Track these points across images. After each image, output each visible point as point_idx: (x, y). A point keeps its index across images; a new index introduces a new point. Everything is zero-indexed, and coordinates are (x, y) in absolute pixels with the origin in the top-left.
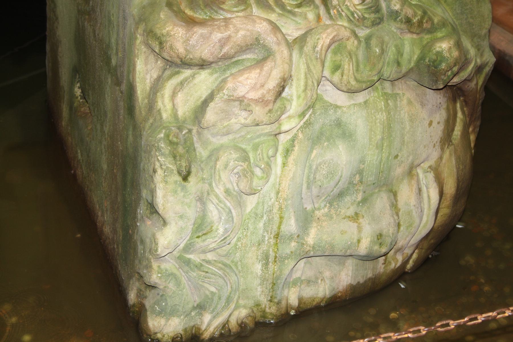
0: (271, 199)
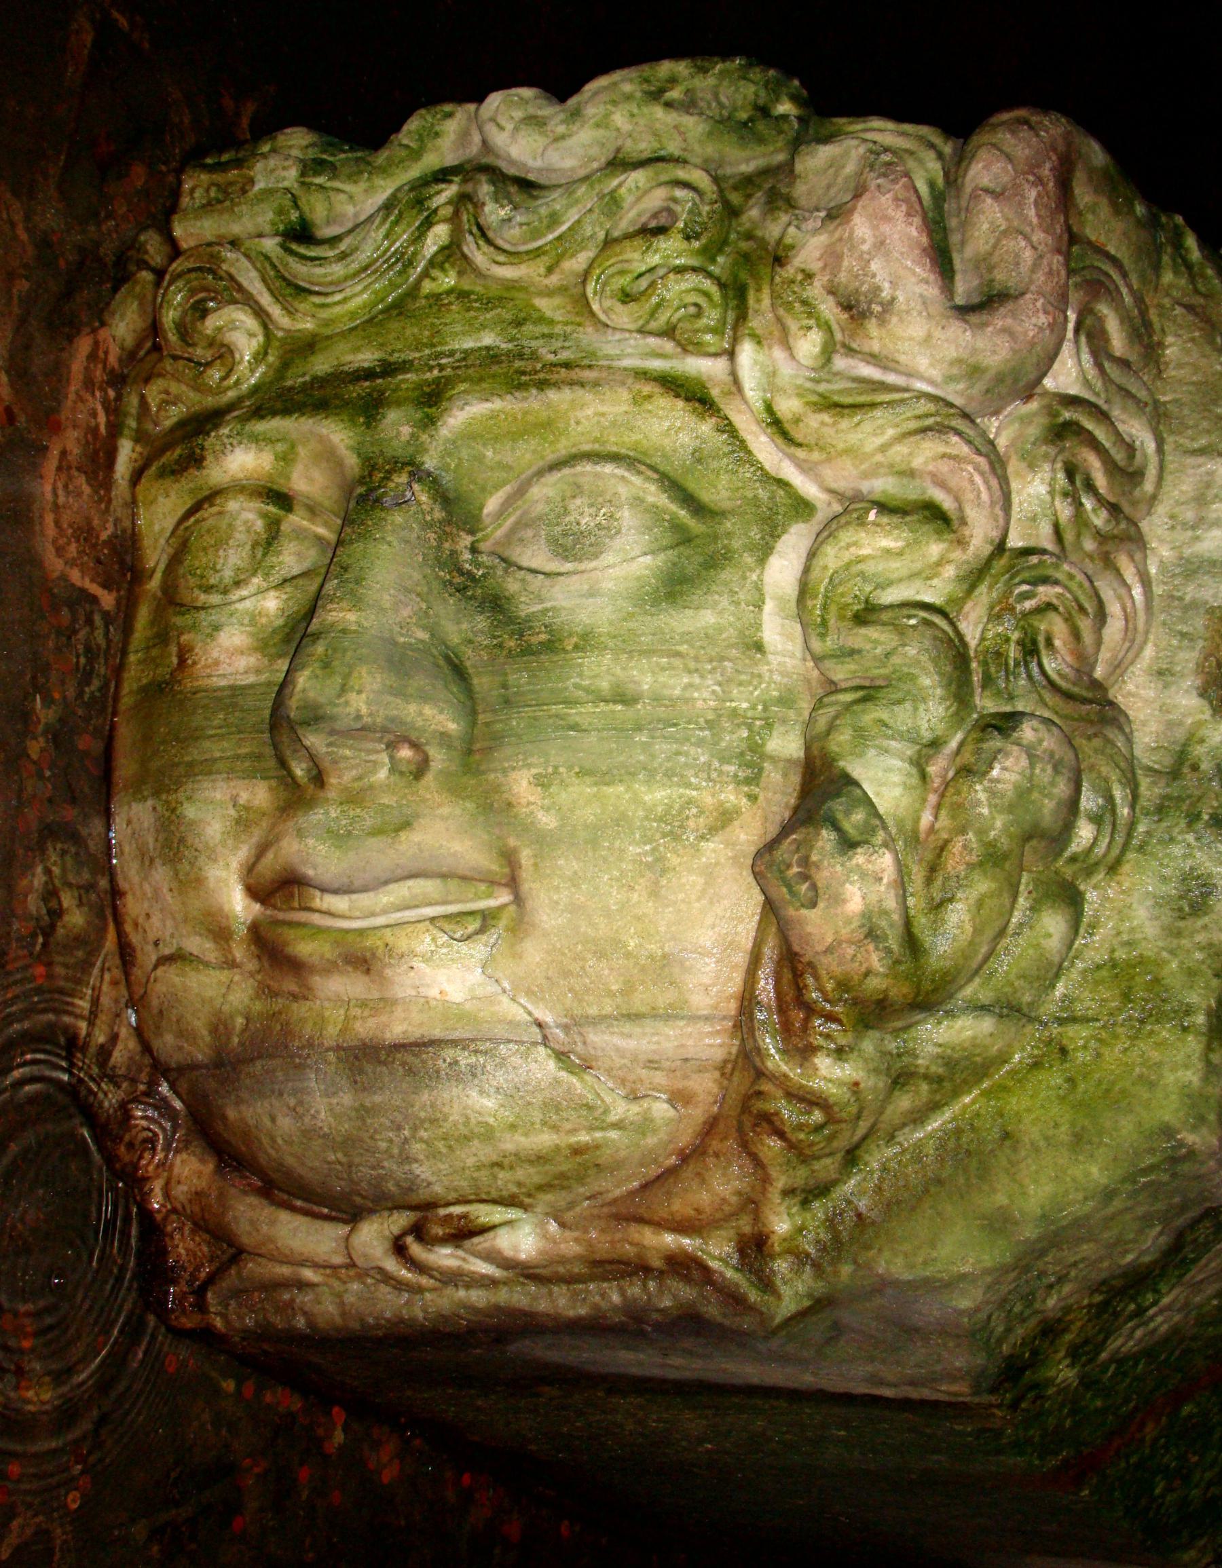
0: (555, 353)
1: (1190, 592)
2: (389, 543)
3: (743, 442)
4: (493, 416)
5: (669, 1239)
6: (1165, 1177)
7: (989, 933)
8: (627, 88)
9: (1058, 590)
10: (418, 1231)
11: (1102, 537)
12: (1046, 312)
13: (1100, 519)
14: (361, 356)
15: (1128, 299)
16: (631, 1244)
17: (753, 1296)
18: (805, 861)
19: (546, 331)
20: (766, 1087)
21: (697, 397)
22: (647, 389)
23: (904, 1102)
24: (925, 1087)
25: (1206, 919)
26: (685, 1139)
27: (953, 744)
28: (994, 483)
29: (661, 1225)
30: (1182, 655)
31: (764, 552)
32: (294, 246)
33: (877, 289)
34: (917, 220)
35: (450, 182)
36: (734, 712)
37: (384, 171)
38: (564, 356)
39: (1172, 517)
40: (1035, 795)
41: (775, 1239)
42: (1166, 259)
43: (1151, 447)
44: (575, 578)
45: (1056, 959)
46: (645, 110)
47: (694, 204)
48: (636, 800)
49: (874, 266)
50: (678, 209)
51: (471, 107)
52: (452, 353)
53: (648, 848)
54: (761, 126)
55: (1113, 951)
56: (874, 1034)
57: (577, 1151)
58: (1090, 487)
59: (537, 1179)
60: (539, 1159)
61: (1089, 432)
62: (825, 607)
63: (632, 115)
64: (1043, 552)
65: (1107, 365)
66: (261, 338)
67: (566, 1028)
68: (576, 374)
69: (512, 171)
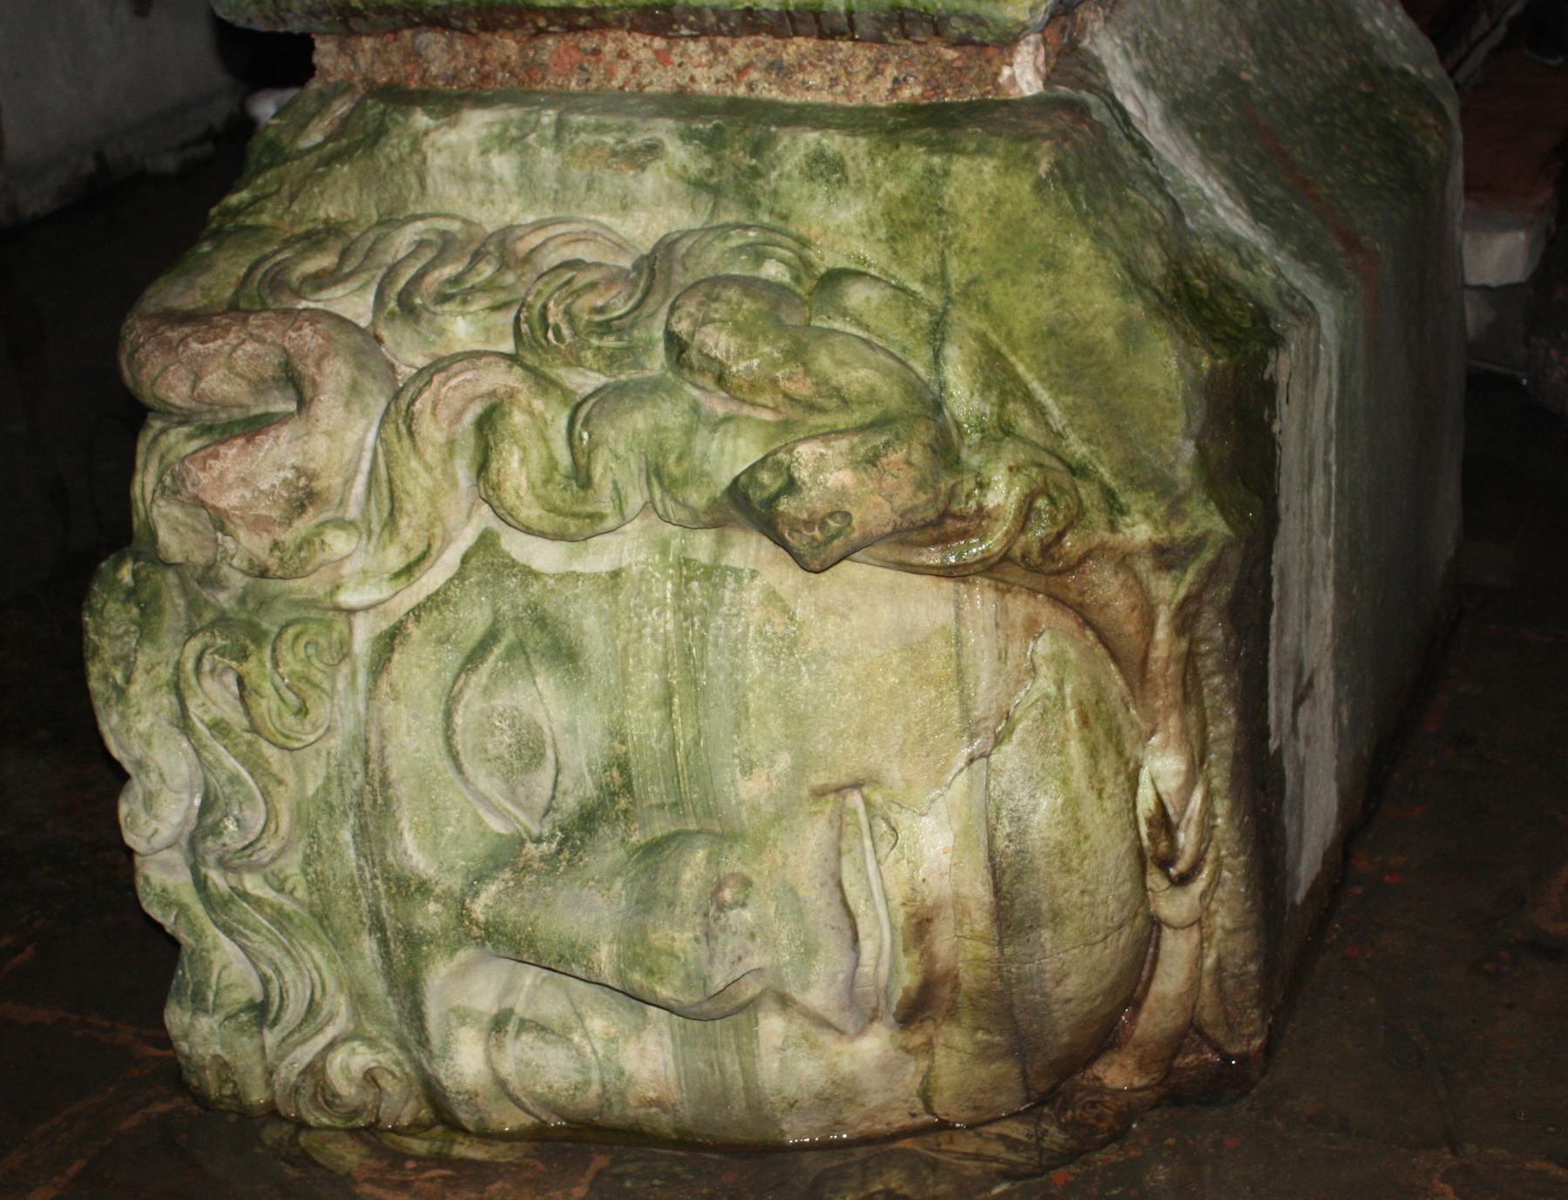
0: (355, 774)
1: (550, 183)
2: (536, 918)
3: (429, 598)
4: (415, 827)
5: (1162, 633)
6: (1081, 187)
7: (867, 352)
8: (115, 719)
9: (551, 304)
10: (1164, 864)
11: (504, 265)
12: (300, 328)
13: (486, 270)
14: (367, 952)
15: (287, 254)
16: (1167, 668)
17: (1208, 555)
18: (809, 524)
19: (336, 783)
20: (1017, 551)
21: (390, 640)
22: (384, 687)
23: (1025, 424)
24: (1011, 406)
25: (847, 158)
26: (1069, 622)
27: (696, 393)
28: (456, 367)
29: (1149, 642)
30: (608, 189)
31: (529, 573)
32: (271, 1016)
33: (285, 482)
34: (223, 449)
35: (206, 877)
36: (677, 595)
37: (199, 936)
38: (358, 766)
39: (482, 203)
40: (740, 318)
41: (1157, 537)
42: (249, 221)
43: (420, 225)
44: (559, 746)
45: (889, 292)
46: (134, 701)
47: (215, 652)
48: (762, 680)
49: (265, 486)
50: (220, 666)
51: (138, 860)
52: (360, 868)
53: (803, 669)
54: (145, 595)
55: (879, 240)
56: (964, 454)
57: (1084, 721)
58: (456, 280)
59: (1112, 757)
60: (1093, 754)
61: (408, 283)
62: (575, 515)
63: (139, 713)
64: (517, 319)
65: (346, 270)
66: (356, 1044)
67: (973, 737)
68: (374, 755)
69: (194, 820)
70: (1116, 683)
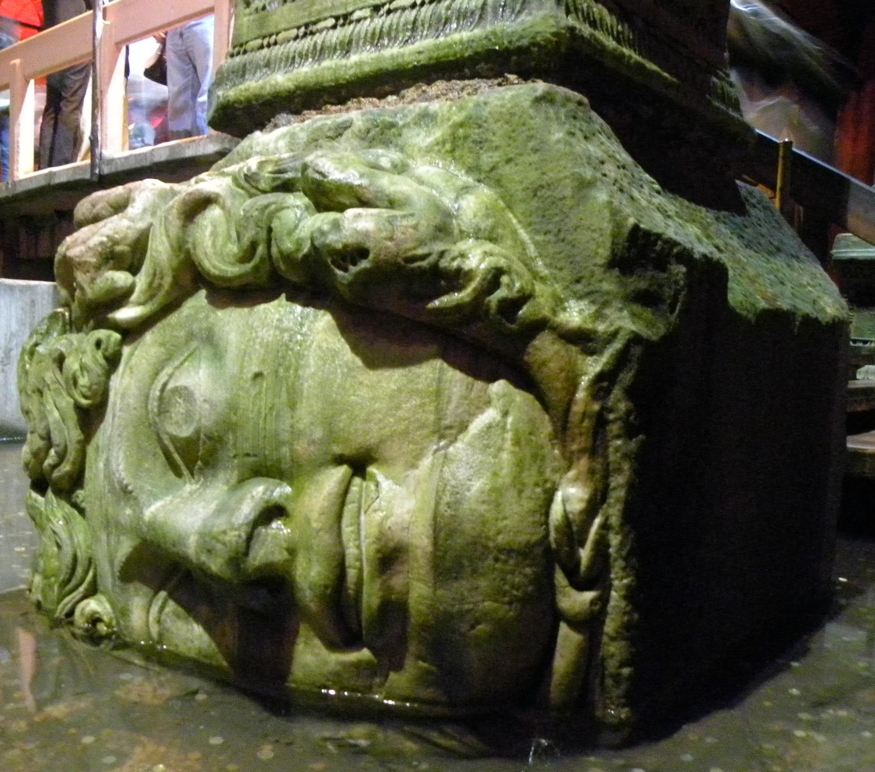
5: (581, 395)
16: (582, 421)
53: (339, 371)
57: (517, 442)
70: (546, 427)
